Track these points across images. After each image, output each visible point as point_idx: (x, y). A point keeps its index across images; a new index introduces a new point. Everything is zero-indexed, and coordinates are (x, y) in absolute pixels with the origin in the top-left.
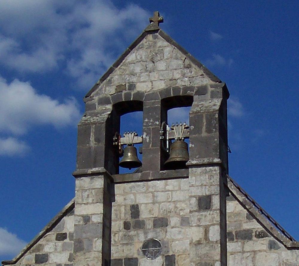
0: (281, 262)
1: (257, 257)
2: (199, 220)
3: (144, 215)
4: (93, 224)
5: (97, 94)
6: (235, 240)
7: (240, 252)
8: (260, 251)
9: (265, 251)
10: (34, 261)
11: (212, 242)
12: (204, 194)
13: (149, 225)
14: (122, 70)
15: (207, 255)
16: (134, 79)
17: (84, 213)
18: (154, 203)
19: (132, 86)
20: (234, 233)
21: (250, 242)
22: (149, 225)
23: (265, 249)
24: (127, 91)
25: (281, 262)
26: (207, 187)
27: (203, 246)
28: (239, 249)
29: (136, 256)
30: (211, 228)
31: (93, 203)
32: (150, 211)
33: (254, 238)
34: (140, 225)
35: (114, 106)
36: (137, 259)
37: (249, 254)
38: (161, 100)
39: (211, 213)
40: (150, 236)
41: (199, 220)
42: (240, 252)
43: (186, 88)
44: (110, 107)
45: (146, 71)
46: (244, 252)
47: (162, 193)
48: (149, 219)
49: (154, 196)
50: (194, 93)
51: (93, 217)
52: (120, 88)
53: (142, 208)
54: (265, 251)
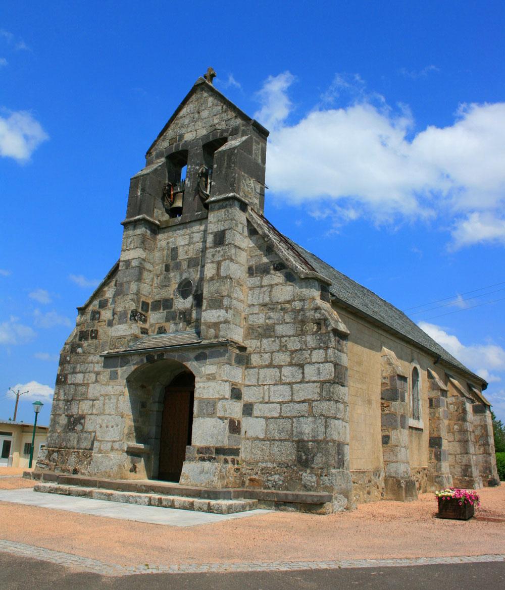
0: (296, 295)
1: (274, 290)
2: (213, 256)
3: (182, 256)
4: (133, 267)
5: (155, 150)
6: (255, 275)
7: (258, 287)
8: (277, 284)
9: (281, 284)
10: (98, 307)
11: (223, 277)
12: (219, 230)
13: (185, 265)
14: (174, 125)
15: (217, 292)
16: (183, 131)
17: (127, 258)
18: (189, 245)
19: (181, 137)
20: (254, 268)
21: (269, 276)
22: (185, 265)
23: (281, 282)
24: (178, 143)
25: (296, 295)
26: (222, 222)
27: (215, 282)
28: (258, 283)
29: (172, 296)
30: (223, 263)
31: (134, 249)
32: (186, 253)
33: (272, 272)
34: (178, 266)
35: (167, 158)
36: (172, 299)
37: (266, 288)
38: (203, 146)
39: (224, 248)
40: (185, 276)
41: (213, 256)
42: (258, 287)
43: (223, 131)
44: (163, 159)
45: (193, 121)
46: (262, 287)
47: (197, 234)
48: (185, 260)
49: (190, 238)
50: (228, 134)
51: (133, 261)
52: (172, 140)
53: (180, 250)
54: (281, 284)
